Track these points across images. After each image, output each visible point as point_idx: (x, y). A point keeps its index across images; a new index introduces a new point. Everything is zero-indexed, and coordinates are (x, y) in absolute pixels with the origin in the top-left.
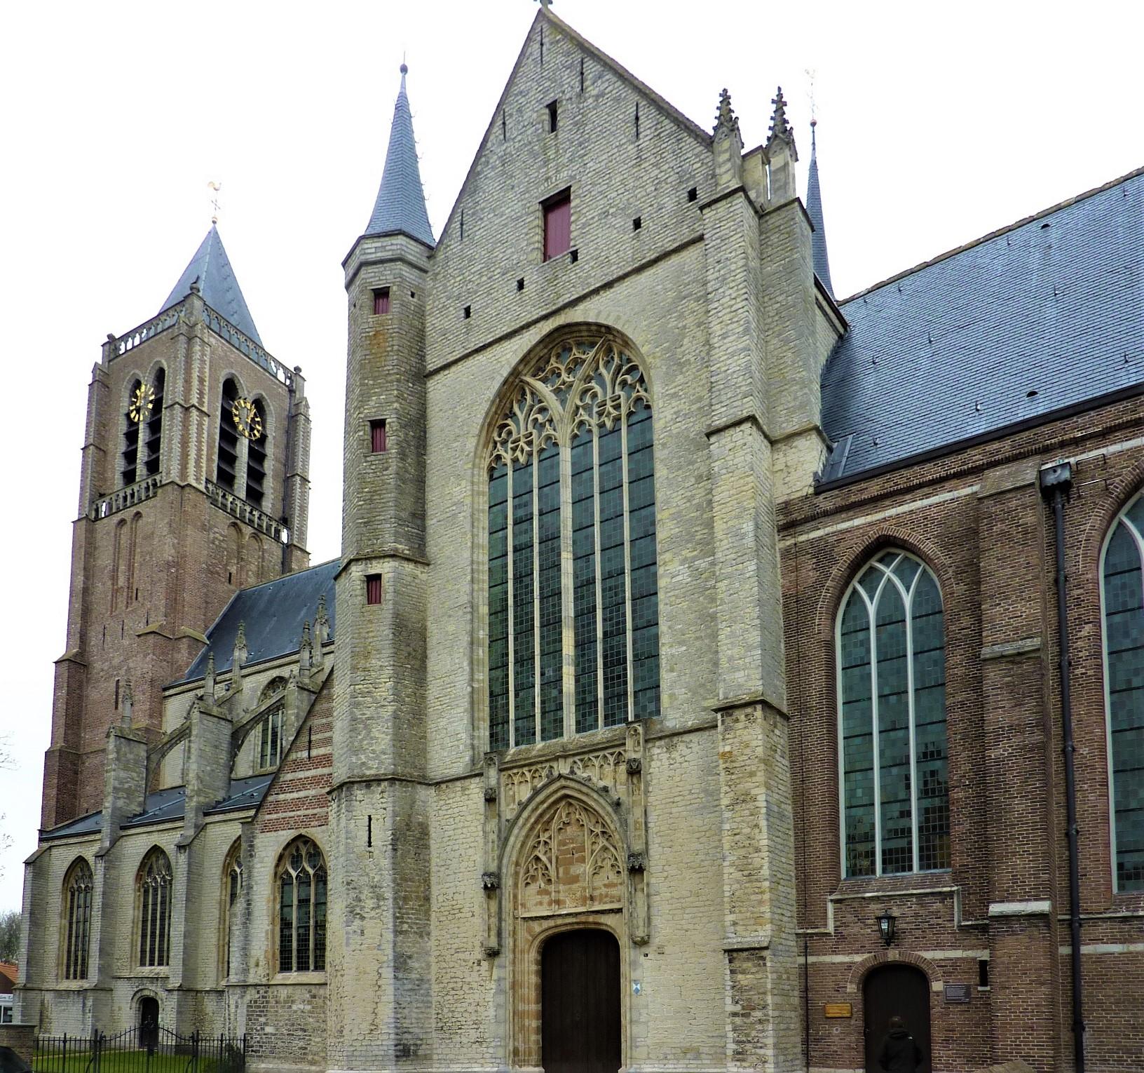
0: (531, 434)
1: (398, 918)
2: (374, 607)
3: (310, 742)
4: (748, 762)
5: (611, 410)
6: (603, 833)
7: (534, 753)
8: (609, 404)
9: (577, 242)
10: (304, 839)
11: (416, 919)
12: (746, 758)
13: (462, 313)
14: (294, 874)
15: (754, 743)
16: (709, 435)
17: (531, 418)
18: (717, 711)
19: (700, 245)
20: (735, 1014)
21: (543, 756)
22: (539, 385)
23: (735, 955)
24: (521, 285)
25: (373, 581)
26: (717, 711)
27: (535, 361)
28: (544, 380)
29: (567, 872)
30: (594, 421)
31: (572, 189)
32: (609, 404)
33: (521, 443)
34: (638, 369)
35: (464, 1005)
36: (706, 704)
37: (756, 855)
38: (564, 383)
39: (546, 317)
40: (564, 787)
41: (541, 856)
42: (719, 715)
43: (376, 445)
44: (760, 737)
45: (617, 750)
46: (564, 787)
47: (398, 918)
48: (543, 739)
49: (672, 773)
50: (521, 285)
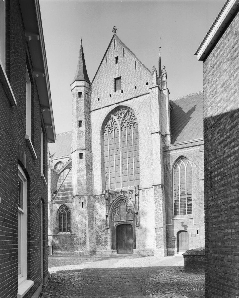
7: (115, 191)
8: (129, 123)
13: (97, 99)
21: (117, 191)
22: (114, 116)
27: (113, 112)
28: (115, 116)
30: (126, 125)
32: (129, 123)
33: (111, 128)
38: (119, 117)
39: (117, 104)
45: (133, 191)
46: (121, 197)
50: (111, 96)
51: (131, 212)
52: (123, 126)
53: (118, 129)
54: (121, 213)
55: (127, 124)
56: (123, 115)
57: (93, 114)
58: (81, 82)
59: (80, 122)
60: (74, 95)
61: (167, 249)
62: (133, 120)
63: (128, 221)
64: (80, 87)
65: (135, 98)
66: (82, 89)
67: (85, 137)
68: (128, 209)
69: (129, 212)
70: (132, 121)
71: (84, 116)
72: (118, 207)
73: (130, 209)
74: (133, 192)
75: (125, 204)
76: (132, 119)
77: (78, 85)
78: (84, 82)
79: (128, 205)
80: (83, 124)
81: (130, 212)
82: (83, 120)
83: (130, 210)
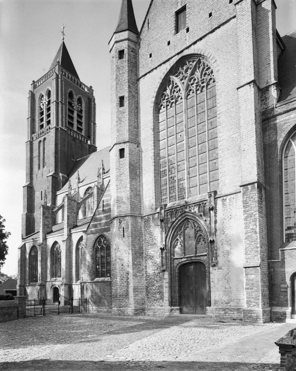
0: (173, 96)
1: (133, 260)
2: (122, 159)
3: (103, 205)
4: (252, 203)
5: (201, 84)
6: (200, 230)
8: (200, 83)
9: (189, 24)
10: (102, 236)
11: (139, 260)
12: (251, 202)
13: (149, 56)
14: (99, 247)
15: (254, 197)
16: (238, 89)
17: (173, 91)
18: (241, 186)
19: (235, 19)
20: (248, 289)
21: (179, 205)
23: (247, 269)
24: (169, 43)
25: (122, 151)
26: (241, 186)
27: (174, 71)
28: (177, 76)
29: (188, 243)
30: (194, 89)
31: (187, 5)
32: (200, 83)
33: (170, 99)
34: (210, 68)
35: (155, 287)
36: (236, 184)
37: (255, 235)
38: (184, 76)
39: (178, 54)
40: (186, 215)
41: (179, 238)
42: (242, 188)
43: (121, 104)
44: (257, 194)
45: (205, 202)
46: (186, 215)
47: (133, 260)
48: (179, 200)
49: (224, 209)
50: (169, 43)
51: (203, 241)
52: (191, 90)
53: (181, 99)
54: (186, 243)
55: (197, 86)
56: (189, 71)
57: (142, 82)
58: (123, 33)
59: (122, 99)
60: (113, 58)
61: (269, 309)
62: (206, 76)
63: (198, 256)
64: (121, 43)
65: (210, 35)
66: (124, 45)
67: (128, 121)
68: (198, 235)
69: (199, 241)
70: (205, 78)
71: (127, 88)
72: (182, 232)
73: (201, 235)
74: (206, 203)
75: (193, 227)
76: (205, 74)
77: (118, 39)
78: (127, 32)
79: (199, 228)
80: (126, 103)
81: (202, 240)
82: (126, 94)
83: (201, 237)
